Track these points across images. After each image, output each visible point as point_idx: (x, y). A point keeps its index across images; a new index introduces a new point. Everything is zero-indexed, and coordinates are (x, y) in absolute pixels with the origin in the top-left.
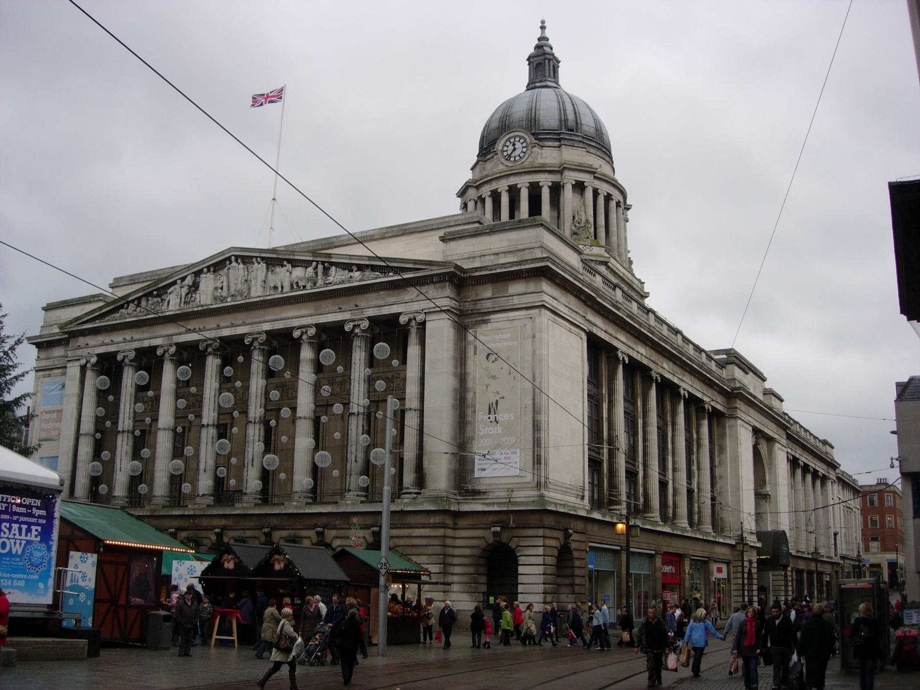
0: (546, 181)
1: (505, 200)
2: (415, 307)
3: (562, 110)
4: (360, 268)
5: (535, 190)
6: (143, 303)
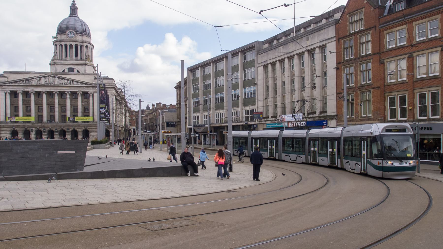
0: (79, 44)
1: (68, 47)
2: (92, 91)
3: (82, 26)
4: (80, 83)
5: (76, 47)
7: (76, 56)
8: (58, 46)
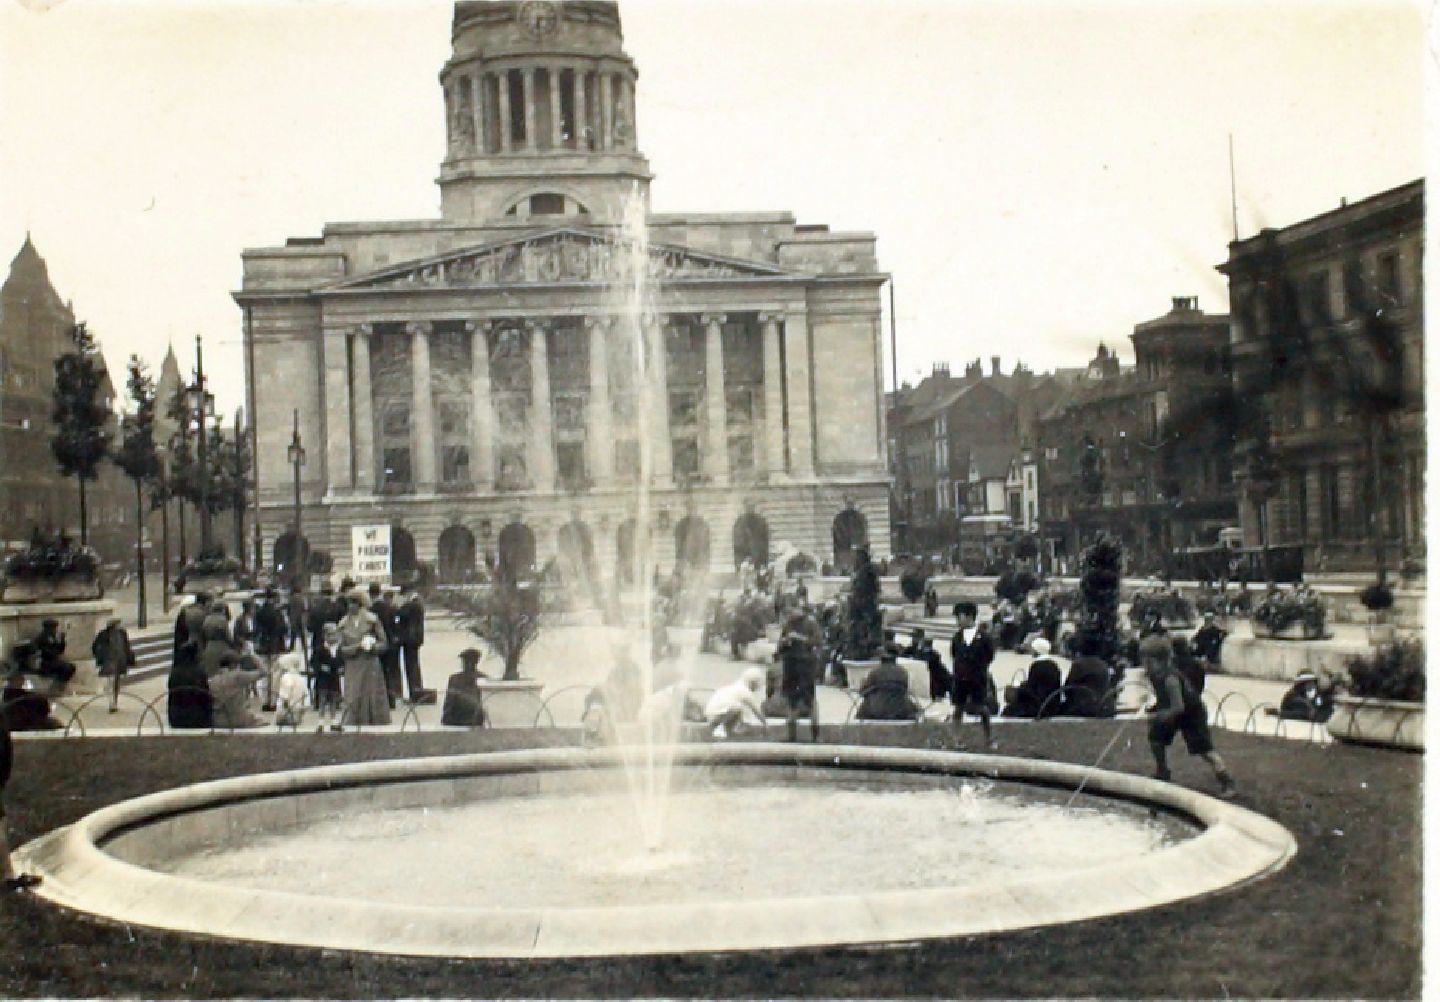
0: (579, 65)
2: (776, 306)
6: (441, 269)
7: (569, 128)
8: (475, 84)
